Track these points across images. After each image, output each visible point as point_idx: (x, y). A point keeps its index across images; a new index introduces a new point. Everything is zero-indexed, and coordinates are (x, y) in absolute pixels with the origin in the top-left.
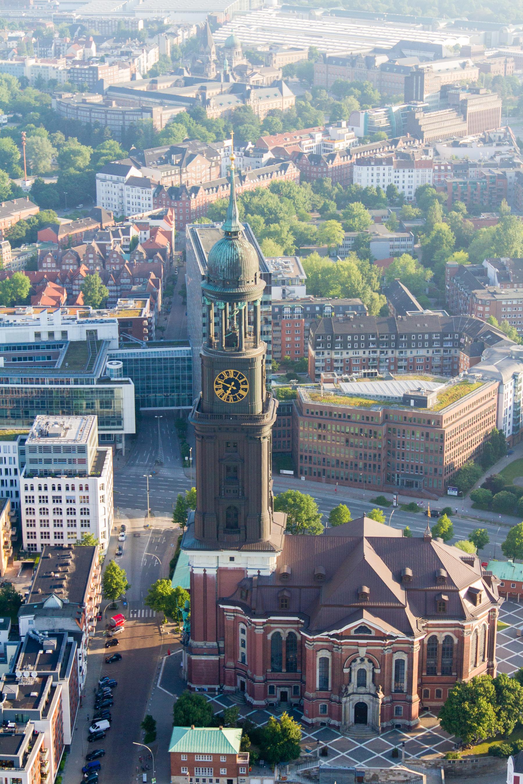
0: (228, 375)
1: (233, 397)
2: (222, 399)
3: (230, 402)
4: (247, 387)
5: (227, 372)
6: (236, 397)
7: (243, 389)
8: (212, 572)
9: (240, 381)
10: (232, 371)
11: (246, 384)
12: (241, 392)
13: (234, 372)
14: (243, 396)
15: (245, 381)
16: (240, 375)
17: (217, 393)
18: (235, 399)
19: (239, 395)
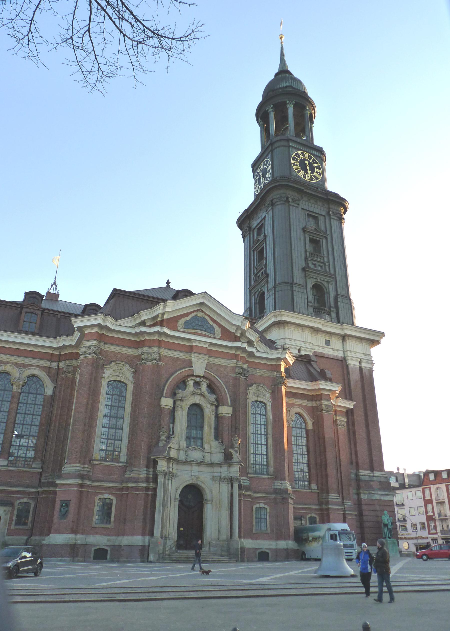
0: (304, 156)
2: (300, 174)
4: (320, 171)
7: (317, 172)
9: (315, 165)
10: (307, 154)
14: (317, 179)
17: (295, 167)
19: (314, 176)
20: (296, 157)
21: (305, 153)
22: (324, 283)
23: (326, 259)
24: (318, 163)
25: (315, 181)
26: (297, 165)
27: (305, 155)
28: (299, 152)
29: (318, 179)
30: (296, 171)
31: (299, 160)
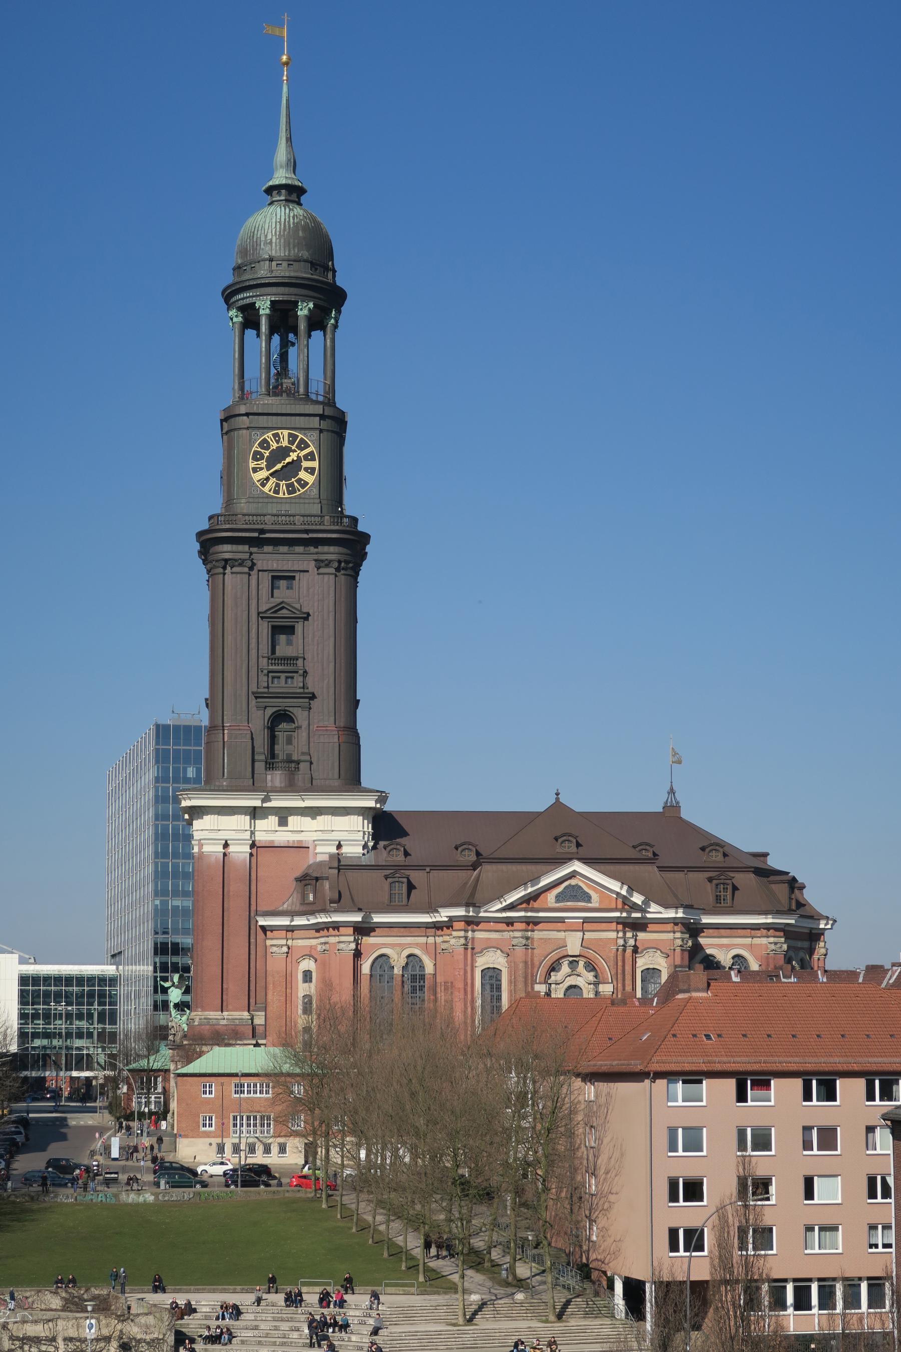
0: (278, 442)
1: (288, 486)
2: (266, 489)
3: (281, 495)
4: (315, 464)
5: (276, 436)
6: (292, 485)
7: (306, 469)
8: (240, 850)
10: (286, 432)
11: (313, 459)
12: (303, 475)
13: (290, 435)
14: (307, 483)
15: (312, 453)
16: (302, 440)
18: (291, 489)
19: (299, 481)
20: (259, 449)
21: (279, 431)
22: (291, 709)
23: (300, 662)
24: (310, 446)
25: (299, 491)
26: (261, 469)
27: (281, 437)
28: (269, 436)
29: (308, 483)
30: (258, 484)
31: (267, 454)
